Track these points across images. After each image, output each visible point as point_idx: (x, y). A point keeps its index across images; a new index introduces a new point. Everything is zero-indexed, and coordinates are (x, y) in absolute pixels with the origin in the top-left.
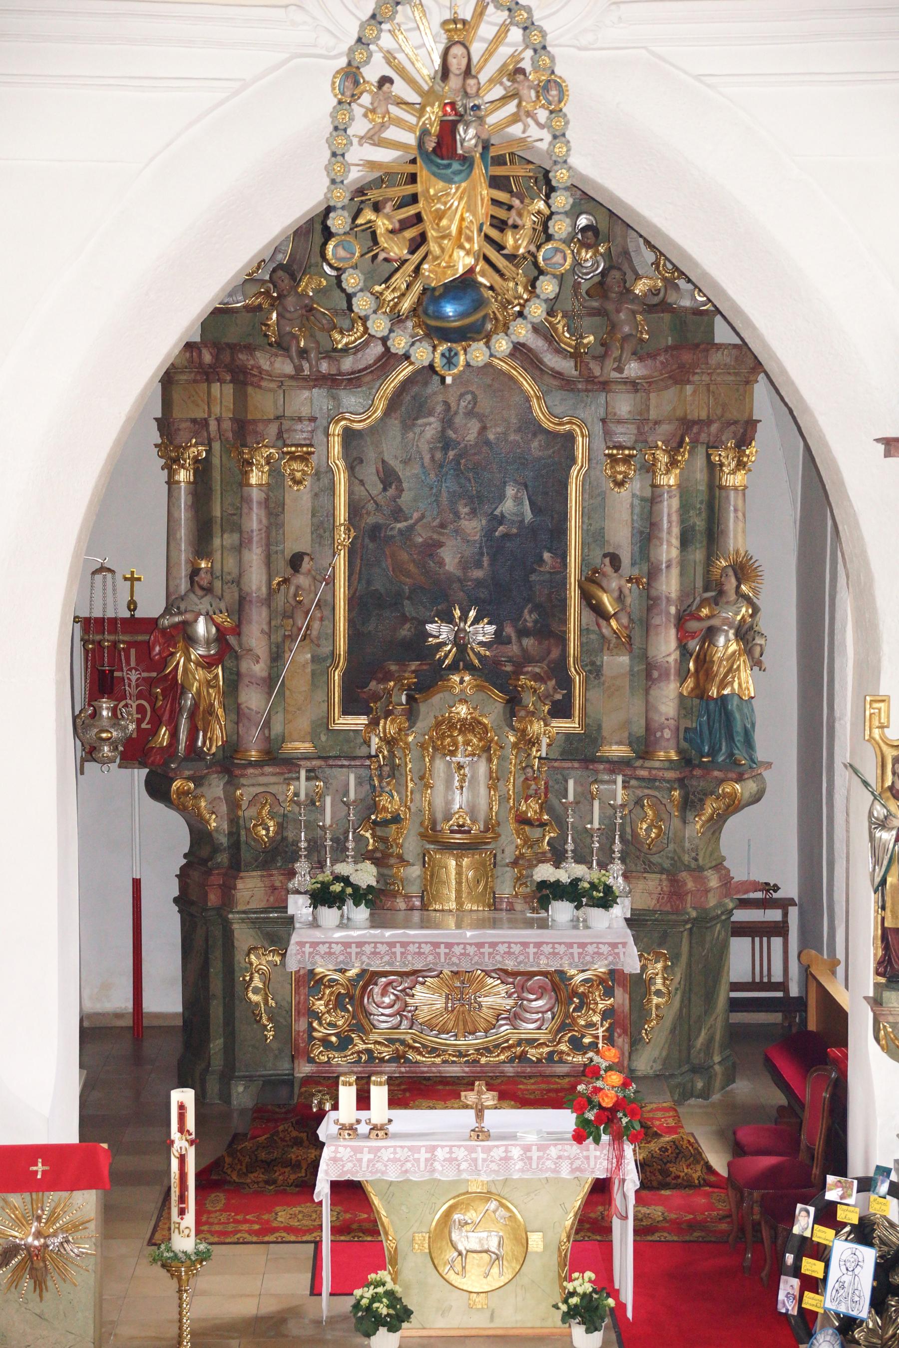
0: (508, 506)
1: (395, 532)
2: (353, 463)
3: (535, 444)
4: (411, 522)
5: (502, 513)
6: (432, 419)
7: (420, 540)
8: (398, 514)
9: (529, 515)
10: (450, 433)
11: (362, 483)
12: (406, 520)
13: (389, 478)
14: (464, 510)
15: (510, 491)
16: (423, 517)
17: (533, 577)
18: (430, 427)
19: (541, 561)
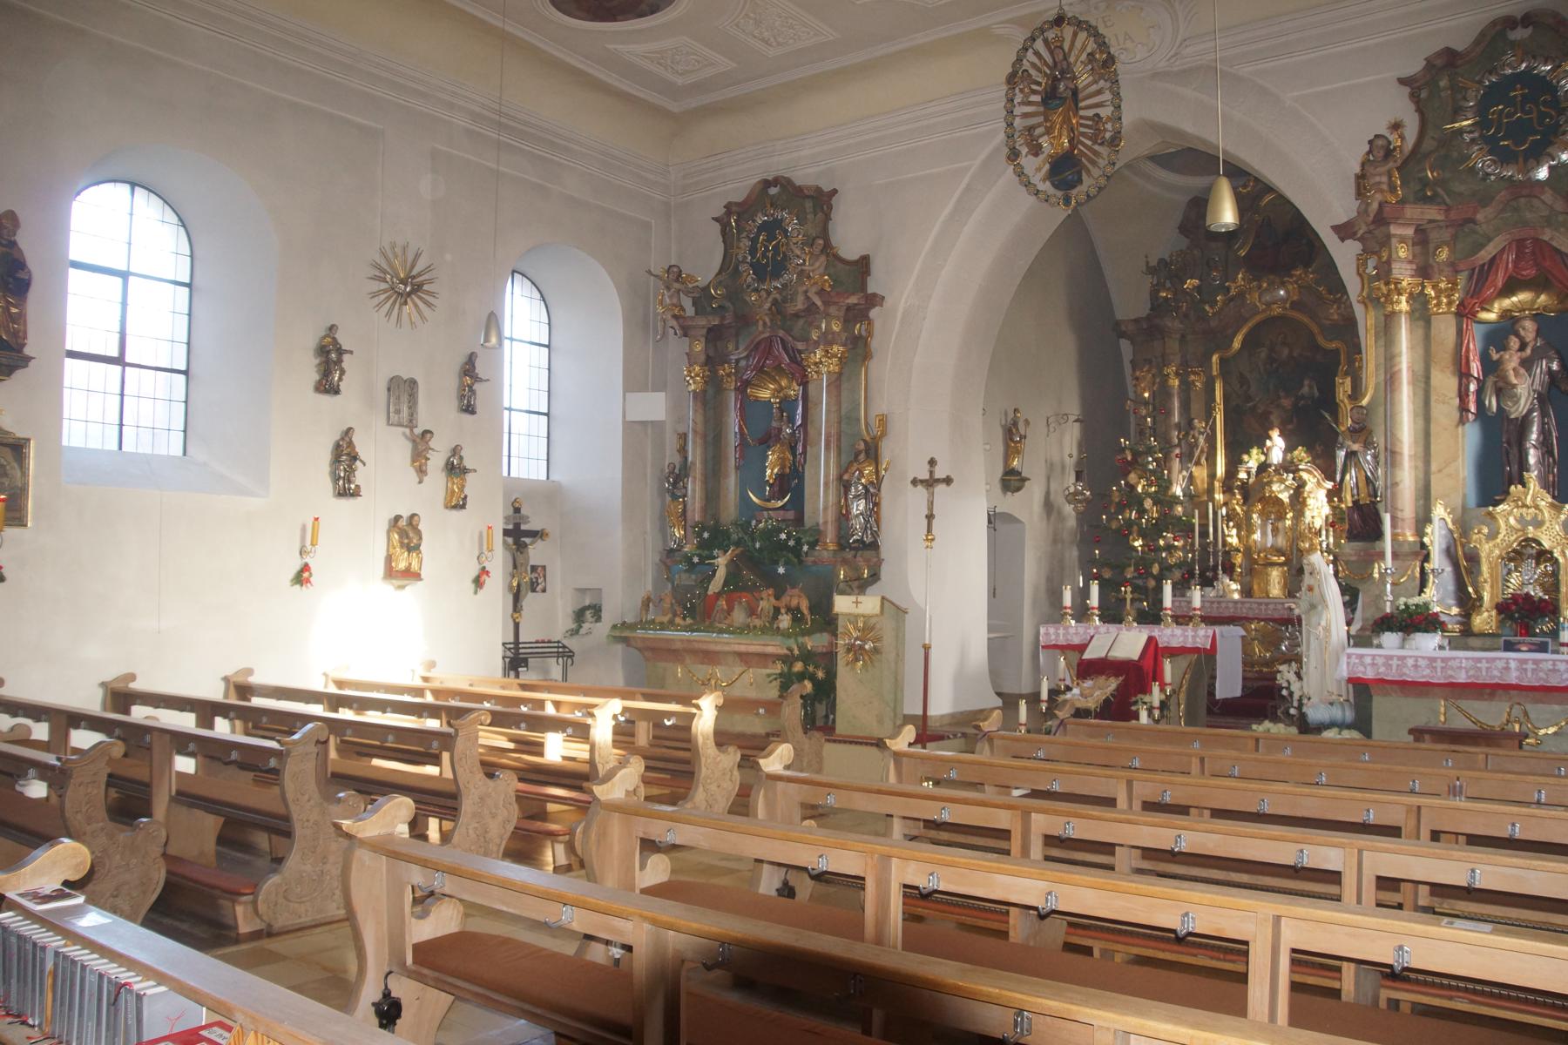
0: (1305, 390)
2: (1225, 374)
8: (1249, 398)
9: (1317, 394)
13: (1243, 380)
15: (1306, 382)
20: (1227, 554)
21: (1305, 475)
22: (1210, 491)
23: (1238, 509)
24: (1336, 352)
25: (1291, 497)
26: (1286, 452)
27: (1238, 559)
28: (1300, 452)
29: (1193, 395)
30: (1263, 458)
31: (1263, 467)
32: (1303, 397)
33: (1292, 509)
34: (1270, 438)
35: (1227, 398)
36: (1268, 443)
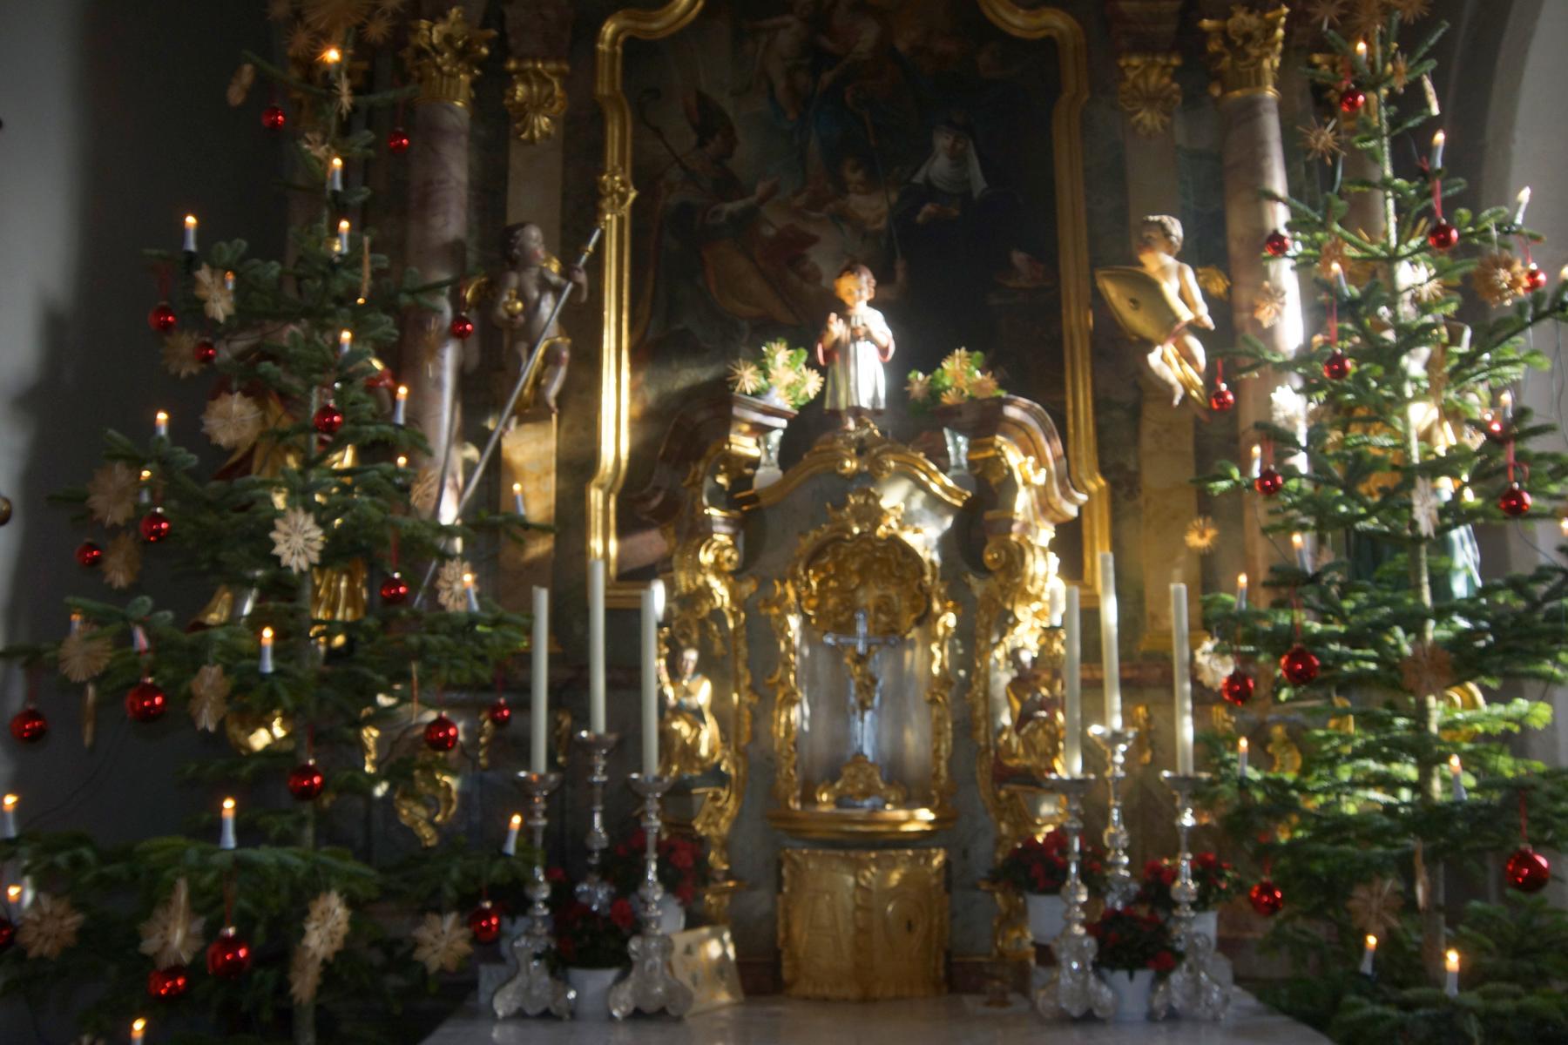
0: (939, 167)
1: (723, 219)
2: (643, 97)
4: (752, 200)
5: (928, 182)
6: (788, 19)
7: (770, 232)
8: (728, 186)
9: (979, 184)
10: (826, 42)
11: (658, 133)
12: (742, 197)
13: (710, 122)
14: (854, 177)
15: (942, 142)
16: (774, 190)
18: (788, 34)
20: (679, 792)
21: (1014, 457)
22: (570, 518)
23: (721, 592)
24: (1048, 46)
25: (945, 543)
26: (898, 369)
27: (717, 816)
28: (962, 373)
29: (517, 160)
30: (812, 383)
31: (812, 425)
32: (929, 191)
33: (958, 596)
34: (843, 311)
35: (643, 177)
36: (837, 328)
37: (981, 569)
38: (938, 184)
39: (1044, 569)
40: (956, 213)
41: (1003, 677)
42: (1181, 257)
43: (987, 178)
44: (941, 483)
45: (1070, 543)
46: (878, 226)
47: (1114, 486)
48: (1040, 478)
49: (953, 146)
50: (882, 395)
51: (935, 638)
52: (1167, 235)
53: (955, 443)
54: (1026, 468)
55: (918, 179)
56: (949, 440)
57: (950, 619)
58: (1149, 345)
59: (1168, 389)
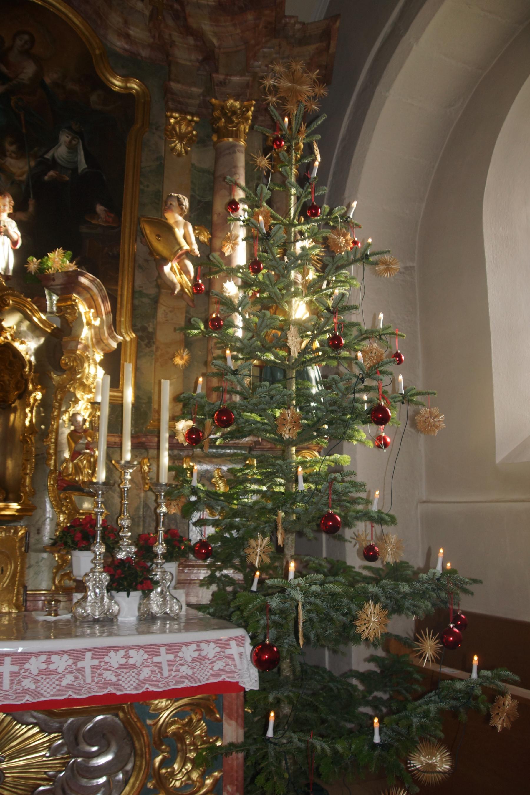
0: (61, 151)
3: (94, 98)
5: (53, 158)
9: (83, 165)
14: (11, 148)
15: (64, 138)
17: (84, 229)
19: (94, 213)
21: (82, 308)
25: (38, 352)
32: (53, 164)
37: (60, 369)
38: (59, 161)
39: (95, 373)
40: (67, 179)
41: (66, 431)
42: (185, 218)
43: (87, 162)
44: (39, 317)
45: (112, 364)
46: (21, 178)
47: (139, 338)
48: (97, 323)
49: (70, 142)
50: (11, 267)
51: (28, 405)
52: (180, 204)
53: (51, 299)
54: (90, 318)
55: (48, 156)
56: (47, 297)
57: (39, 395)
58: (165, 261)
59: (174, 285)
